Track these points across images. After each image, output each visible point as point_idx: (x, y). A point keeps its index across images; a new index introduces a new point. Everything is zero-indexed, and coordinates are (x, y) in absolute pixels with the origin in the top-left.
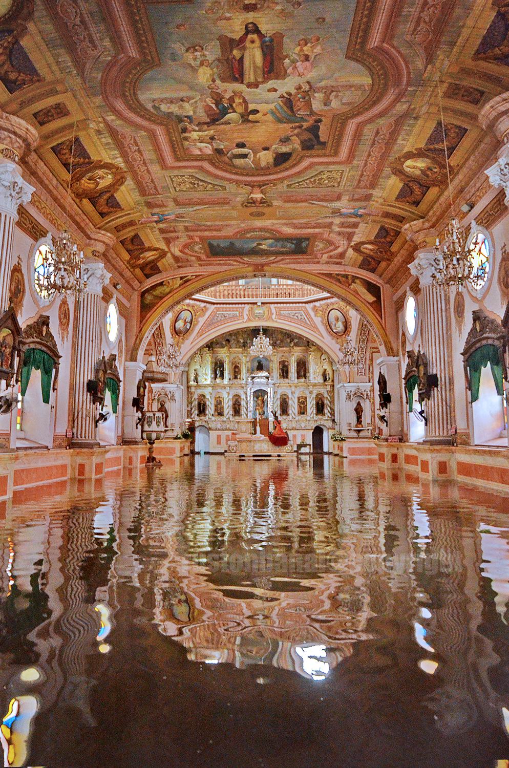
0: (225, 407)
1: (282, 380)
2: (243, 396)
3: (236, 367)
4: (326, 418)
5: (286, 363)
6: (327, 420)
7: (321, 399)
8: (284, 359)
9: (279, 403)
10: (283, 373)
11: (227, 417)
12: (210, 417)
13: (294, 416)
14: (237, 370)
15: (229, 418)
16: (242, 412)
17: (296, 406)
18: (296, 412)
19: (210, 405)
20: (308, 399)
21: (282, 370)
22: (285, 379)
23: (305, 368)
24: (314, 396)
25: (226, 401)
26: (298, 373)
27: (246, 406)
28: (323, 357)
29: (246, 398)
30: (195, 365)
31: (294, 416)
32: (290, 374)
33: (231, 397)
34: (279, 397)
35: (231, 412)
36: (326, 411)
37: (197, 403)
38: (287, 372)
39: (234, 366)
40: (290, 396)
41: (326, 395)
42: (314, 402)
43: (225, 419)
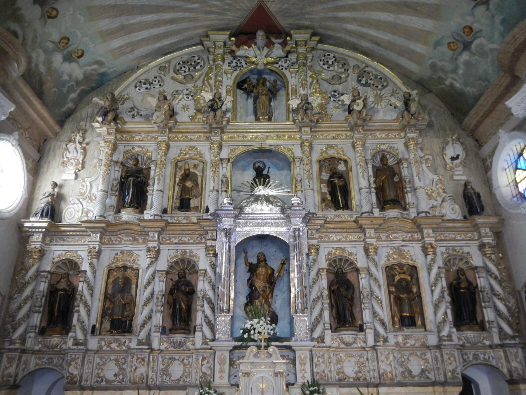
0: (141, 297)
1: (331, 214)
2: (203, 264)
3: (187, 176)
4: (496, 340)
5: (341, 167)
6: (502, 346)
7: (460, 272)
8: (332, 153)
9: (324, 283)
10: (333, 192)
11: (143, 335)
12: (80, 336)
13: (381, 330)
14: (189, 184)
15: (148, 342)
16: (199, 319)
17: (382, 294)
18: (385, 314)
19: (86, 293)
20: (423, 275)
21: (331, 184)
22: (340, 212)
23: (401, 180)
24: (440, 262)
25: (144, 277)
26: (380, 191)
27: (210, 294)
28: (450, 152)
29: (214, 266)
30: (62, 172)
31: (381, 330)
32: (355, 198)
33: (163, 265)
34: (323, 263)
35: (158, 319)
36: (489, 315)
37: (43, 287)
38: (346, 191)
39: (180, 173)
40: (361, 262)
41: (477, 260)
42: (443, 283)
43: (133, 345)
